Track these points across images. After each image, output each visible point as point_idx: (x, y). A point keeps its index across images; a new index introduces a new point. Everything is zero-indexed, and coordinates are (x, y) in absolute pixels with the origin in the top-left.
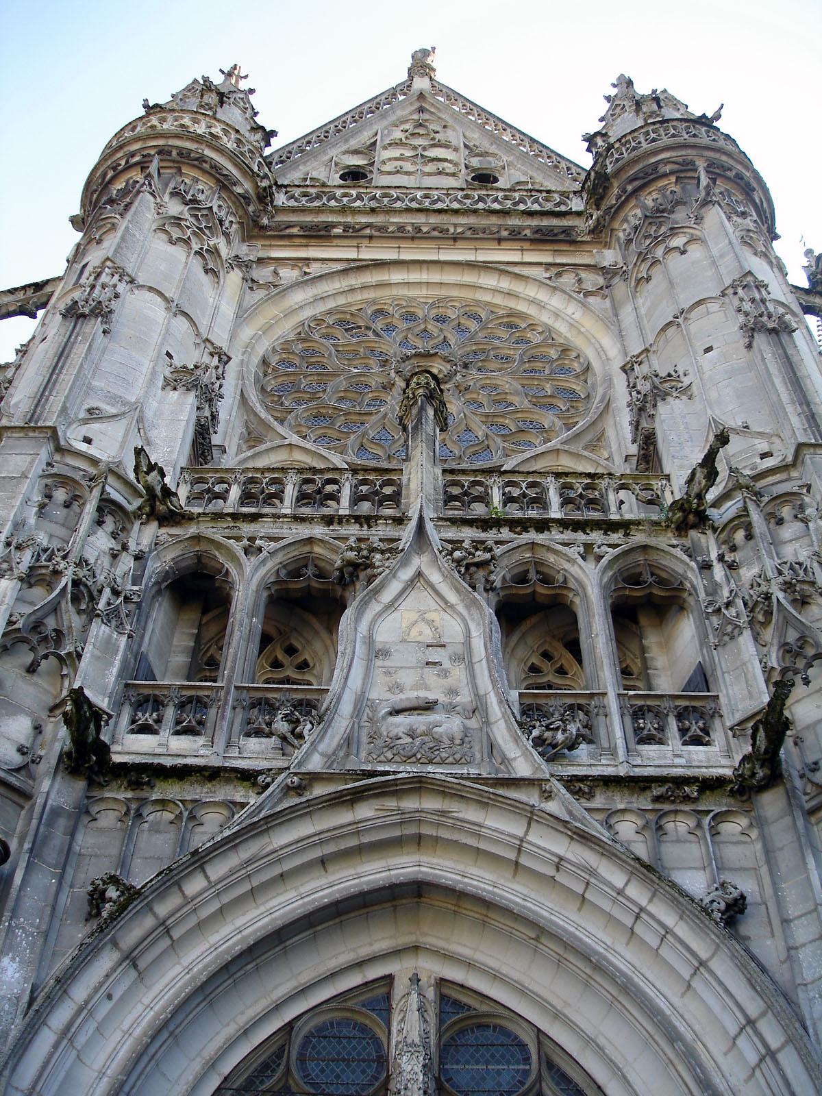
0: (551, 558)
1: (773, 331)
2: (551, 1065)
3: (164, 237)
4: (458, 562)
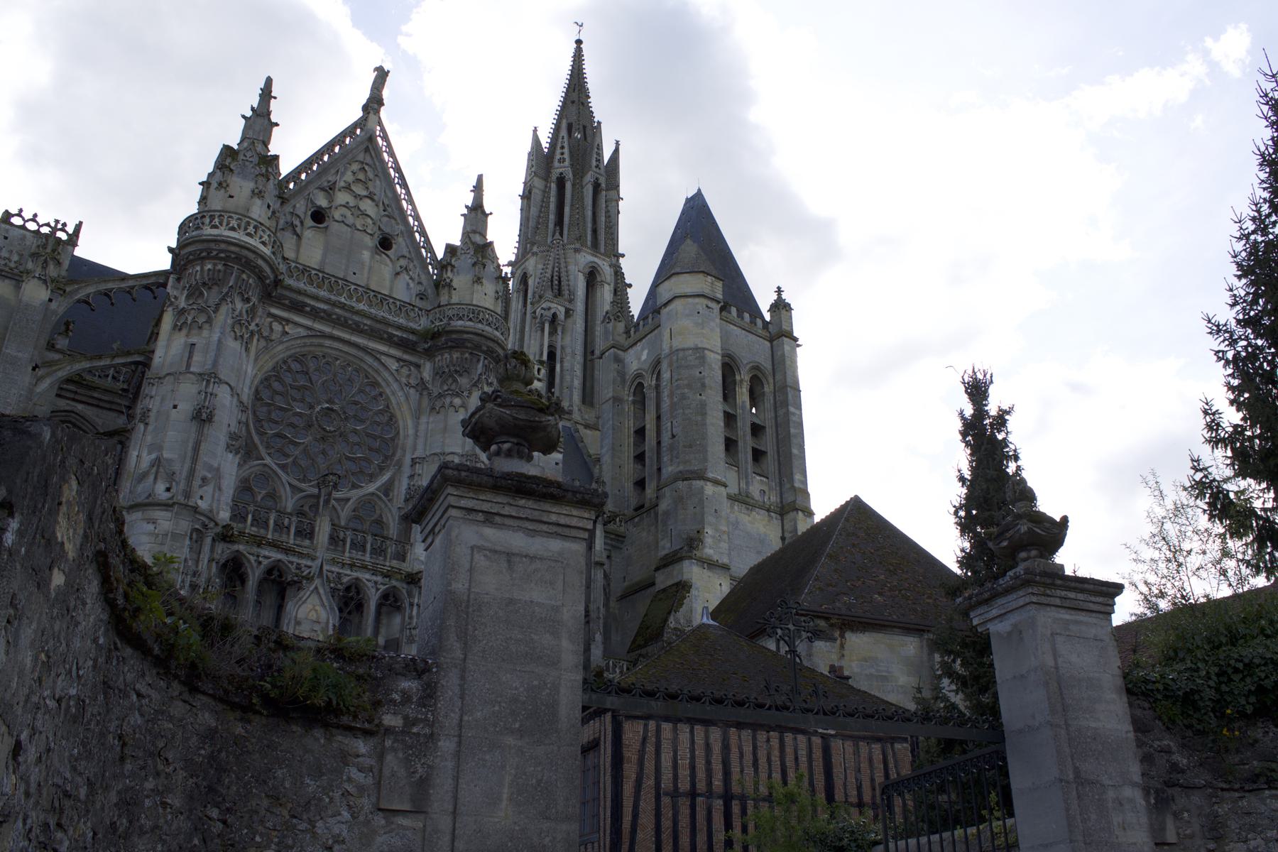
3: (232, 334)
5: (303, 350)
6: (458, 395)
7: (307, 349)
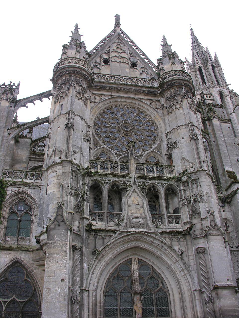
0: (155, 186)
1: (195, 139)
2: (153, 271)
3: (77, 98)
4: (141, 188)
5: (110, 105)
6: (177, 103)
7: (111, 104)
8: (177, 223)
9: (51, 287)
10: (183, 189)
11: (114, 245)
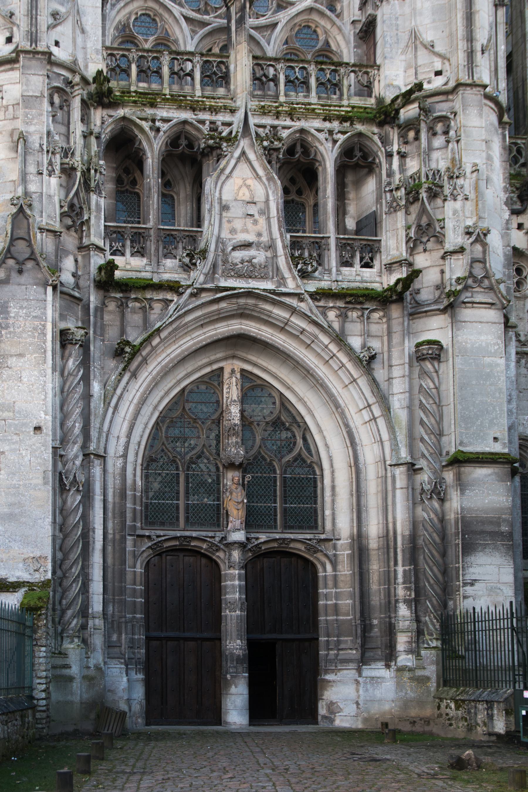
8: (367, 265)
9: (6, 448)
10: (399, 153)
11: (175, 329)
